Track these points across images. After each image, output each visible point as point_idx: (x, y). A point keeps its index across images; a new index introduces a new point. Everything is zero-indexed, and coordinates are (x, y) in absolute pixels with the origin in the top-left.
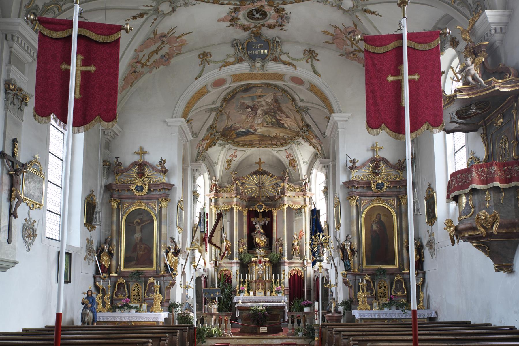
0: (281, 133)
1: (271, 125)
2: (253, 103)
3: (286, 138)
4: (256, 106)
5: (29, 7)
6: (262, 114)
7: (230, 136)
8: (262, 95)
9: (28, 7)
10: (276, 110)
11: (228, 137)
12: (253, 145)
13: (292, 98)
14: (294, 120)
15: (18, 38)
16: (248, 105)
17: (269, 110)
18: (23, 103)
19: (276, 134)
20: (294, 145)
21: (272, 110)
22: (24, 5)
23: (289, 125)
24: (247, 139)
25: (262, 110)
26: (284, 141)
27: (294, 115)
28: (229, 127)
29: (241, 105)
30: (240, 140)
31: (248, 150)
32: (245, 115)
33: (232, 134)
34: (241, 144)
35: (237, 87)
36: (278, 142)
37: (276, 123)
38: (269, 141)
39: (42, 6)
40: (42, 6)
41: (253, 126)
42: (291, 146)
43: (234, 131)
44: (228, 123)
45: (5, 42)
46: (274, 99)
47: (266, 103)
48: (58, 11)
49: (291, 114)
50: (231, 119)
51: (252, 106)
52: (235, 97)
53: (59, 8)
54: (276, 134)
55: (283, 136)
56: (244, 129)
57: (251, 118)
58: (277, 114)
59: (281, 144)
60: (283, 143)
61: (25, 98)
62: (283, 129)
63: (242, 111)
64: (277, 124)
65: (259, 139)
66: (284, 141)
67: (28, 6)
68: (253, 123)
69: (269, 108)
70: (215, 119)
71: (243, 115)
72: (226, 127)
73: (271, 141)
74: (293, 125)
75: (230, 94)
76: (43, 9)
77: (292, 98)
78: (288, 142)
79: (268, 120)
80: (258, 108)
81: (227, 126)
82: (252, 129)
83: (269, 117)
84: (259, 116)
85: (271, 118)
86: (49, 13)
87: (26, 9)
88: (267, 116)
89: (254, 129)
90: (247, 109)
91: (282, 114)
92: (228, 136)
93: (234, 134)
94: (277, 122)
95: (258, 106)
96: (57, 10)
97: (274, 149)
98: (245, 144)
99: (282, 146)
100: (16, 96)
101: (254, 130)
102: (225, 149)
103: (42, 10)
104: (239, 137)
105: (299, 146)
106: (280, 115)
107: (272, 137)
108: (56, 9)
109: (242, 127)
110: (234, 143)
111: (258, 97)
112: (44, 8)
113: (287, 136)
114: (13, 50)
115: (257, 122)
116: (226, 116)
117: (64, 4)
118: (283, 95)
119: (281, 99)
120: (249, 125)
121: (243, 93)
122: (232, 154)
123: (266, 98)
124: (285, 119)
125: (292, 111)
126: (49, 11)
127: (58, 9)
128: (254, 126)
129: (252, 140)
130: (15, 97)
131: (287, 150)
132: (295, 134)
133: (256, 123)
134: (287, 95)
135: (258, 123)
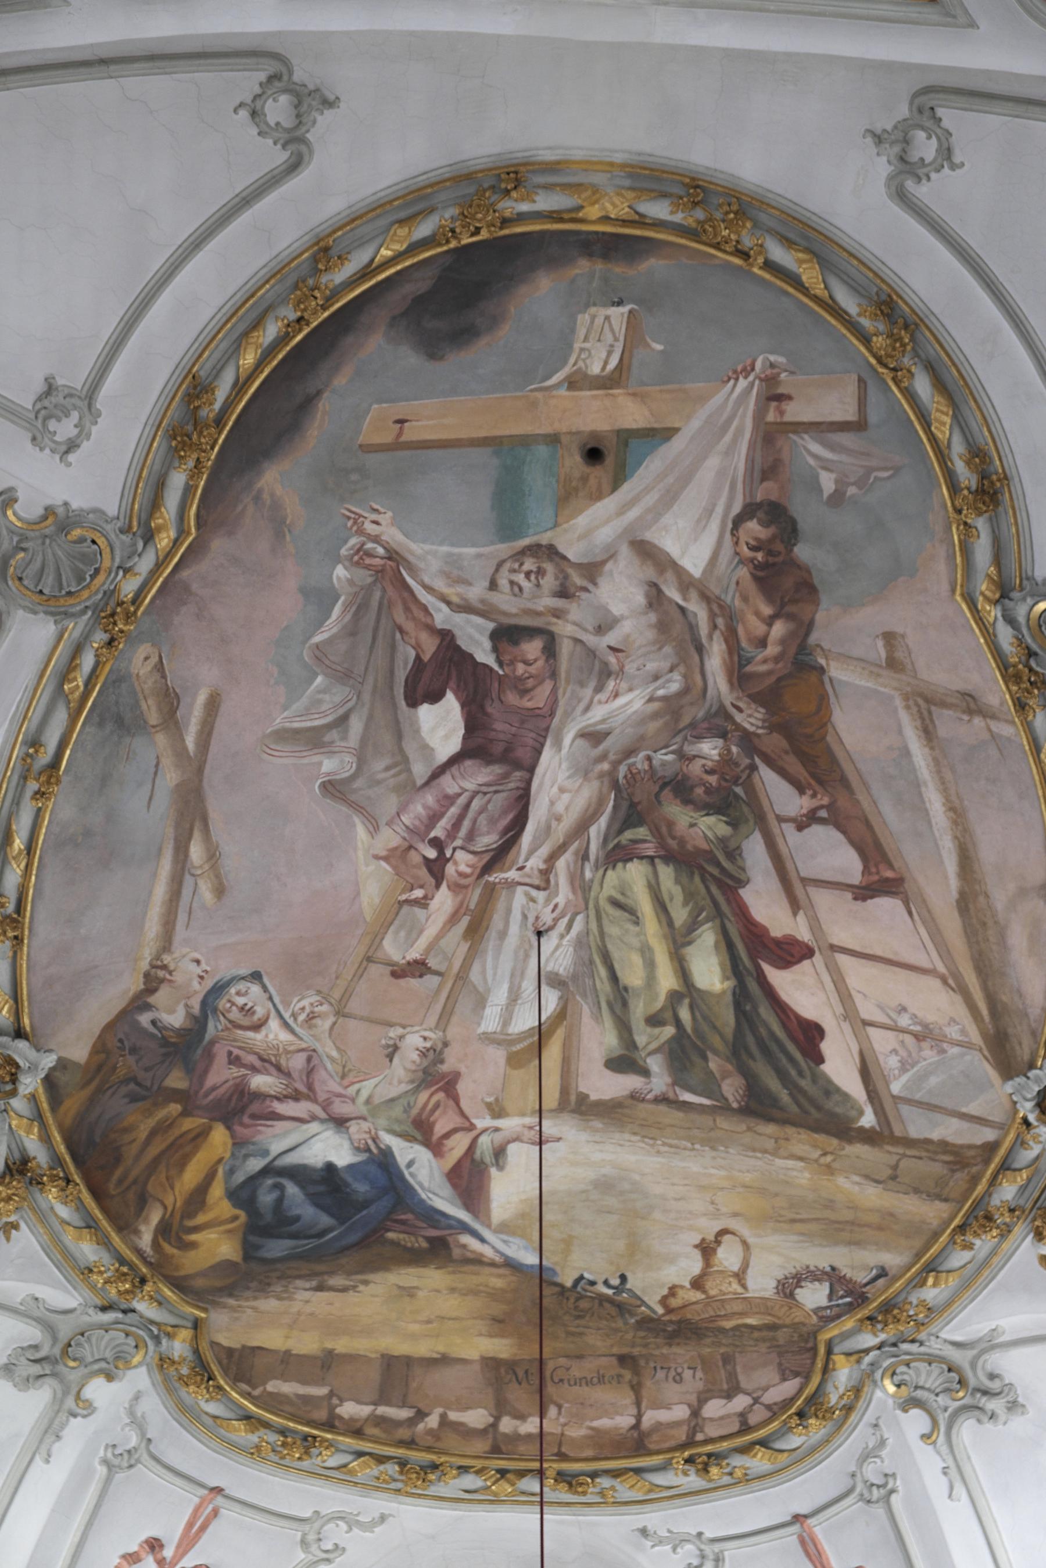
0: (764, 1220)
1: (660, 1081)
2: (505, 602)
3: (827, 1317)
4: (532, 648)
6: (582, 827)
7: (164, 1230)
8: (625, 437)
10: (747, 740)
11: (146, 1239)
12: (410, 1443)
13: (978, 456)
14: (952, 924)
16: (442, 616)
17: (664, 757)
19: (695, 1265)
20: (916, 1421)
21: (710, 749)
23: (882, 1042)
24: (361, 1345)
25: (594, 737)
26: (790, 1387)
27: (957, 814)
28: (176, 1019)
29: (359, 608)
30: (273, 1339)
31: (351, 1522)
32: (390, 838)
33: (191, 1176)
34: (274, 1402)
35: (355, 219)
36: (714, 1408)
37: (727, 1018)
38: (600, 1394)
41: (449, 1085)
42: (866, 1456)
43: (219, 1135)
44: (167, 942)
46: (749, 511)
47: (655, 597)
49: (922, 810)
50: (213, 855)
51: (484, 655)
52: (308, 403)
54: (695, 1265)
55: (788, 1287)
56: (340, 1123)
57: (443, 900)
58: (761, 820)
59: (745, 1428)
60: (775, 1410)
62: (802, 1142)
63: (356, 725)
64: (737, 1052)
65: (501, 1348)
66: (790, 1387)
68: (454, 1031)
69: (672, 706)
70: (35, 743)
71: (361, 832)
72: (140, 1003)
73: (628, 1399)
74: (924, 1034)
75: (258, 324)
77: (978, 456)
78: (843, 1375)
79: (633, 976)
80: (539, 698)
81: (152, 983)
82: (436, 1149)
83: (661, 906)
84: (545, 880)
85: (680, 915)
88: (635, 873)
89: (458, 1146)
90: (426, 712)
91: (811, 819)
92: (142, 1202)
93: (217, 1191)
94: (740, 997)
95: (550, 650)
97: (654, 1518)
98: (330, 1424)
99: (758, 1462)
101: (454, 1175)
102: (77, 1431)
104: (264, 1288)
105: (967, 1430)
106: (791, 838)
107: (648, 1324)
109: (327, 1083)
110: (202, 1372)
111: (574, 461)
113: (833, 1276)
115: (514, 997)
116: (170, 777)
118: (859, 426)
119: (837, 499)
120: (414, 1041)
121: (409, 358)
122: (154, 1545)
123: (669, 499)
124: (840, 936)
125: (947, 724)
128: (463, 1088)
129: (408, 1361)
131: (819, 1527)
132: (933, 1212)
133: (490, 1021)
134: (922, 386)
135: (525, 1021)
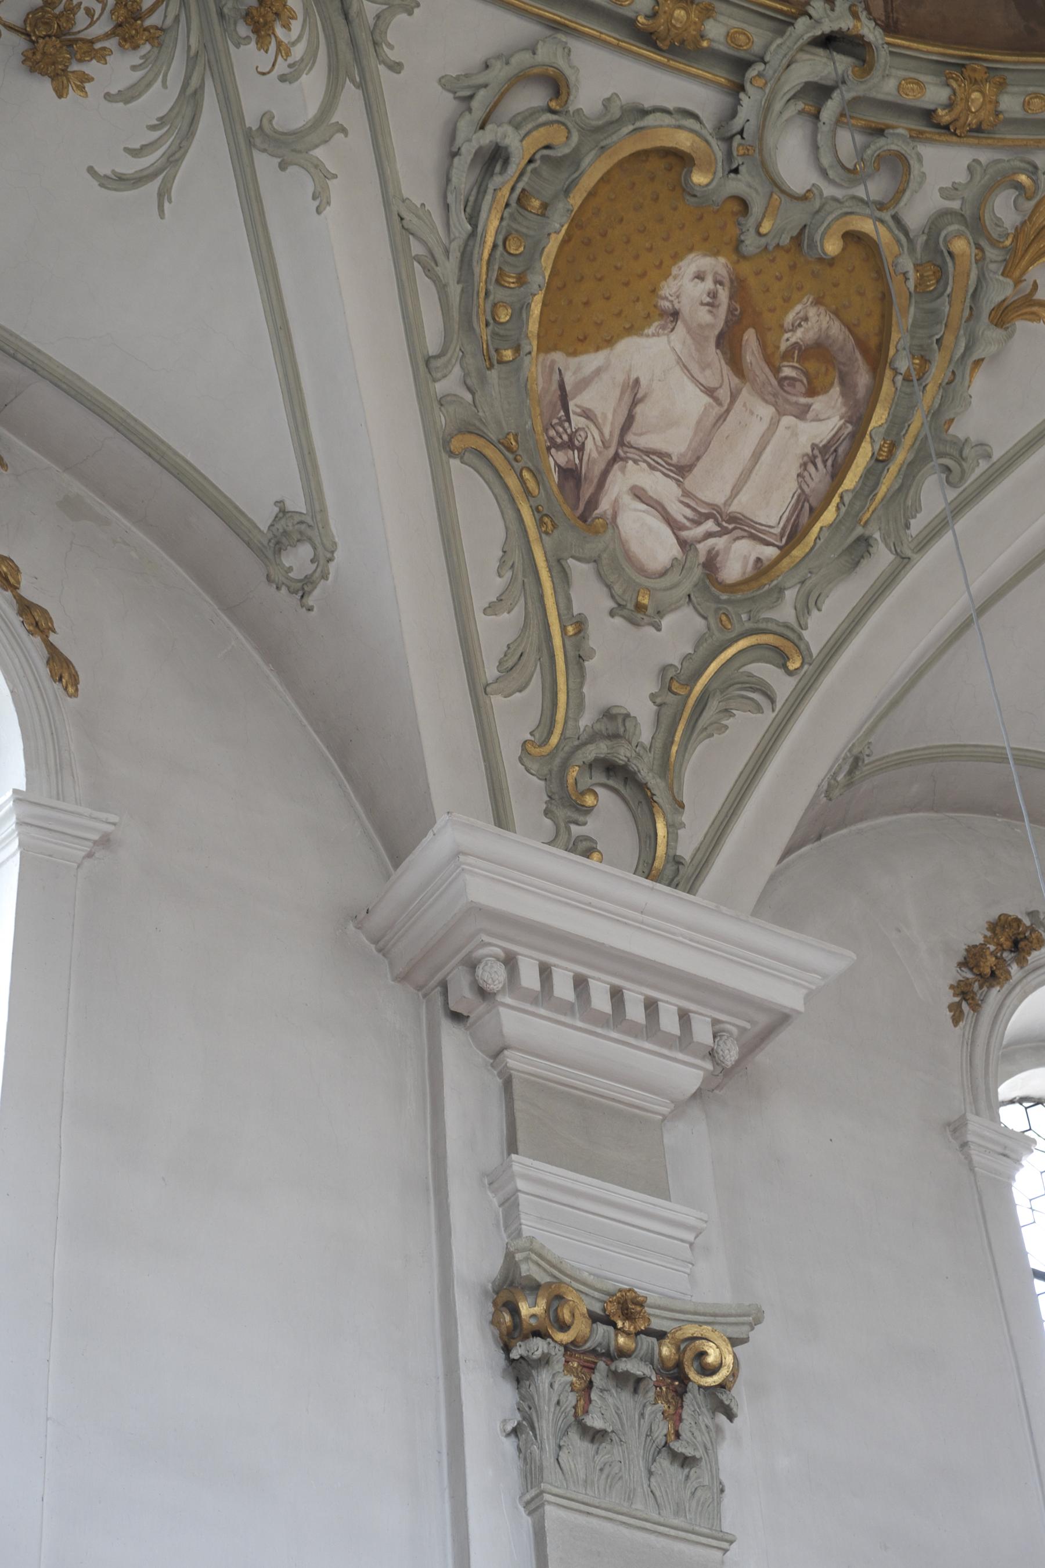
5: (554, 740)
9: (546, 750)
15: (510, 962)
18: (688, 1398)
22: (509, 751)
39: (653, 697)
40: (653, 697)
45: (451, 1036)
48: (790, 673)
53: (776, 649)
61: (689, 1355)
67: (545, 742)
76: (668, 712)
86: (727, 712)
87: (534, 767)
96: (780, 672)
100: (601, 1365)
103: (665, 722)
108: (765, 671)
112: (670, 698)
114: (513, 1060)
117: (807, 605)
126: (714, 706)
127: (781, 659)
130: (598, 1379)
